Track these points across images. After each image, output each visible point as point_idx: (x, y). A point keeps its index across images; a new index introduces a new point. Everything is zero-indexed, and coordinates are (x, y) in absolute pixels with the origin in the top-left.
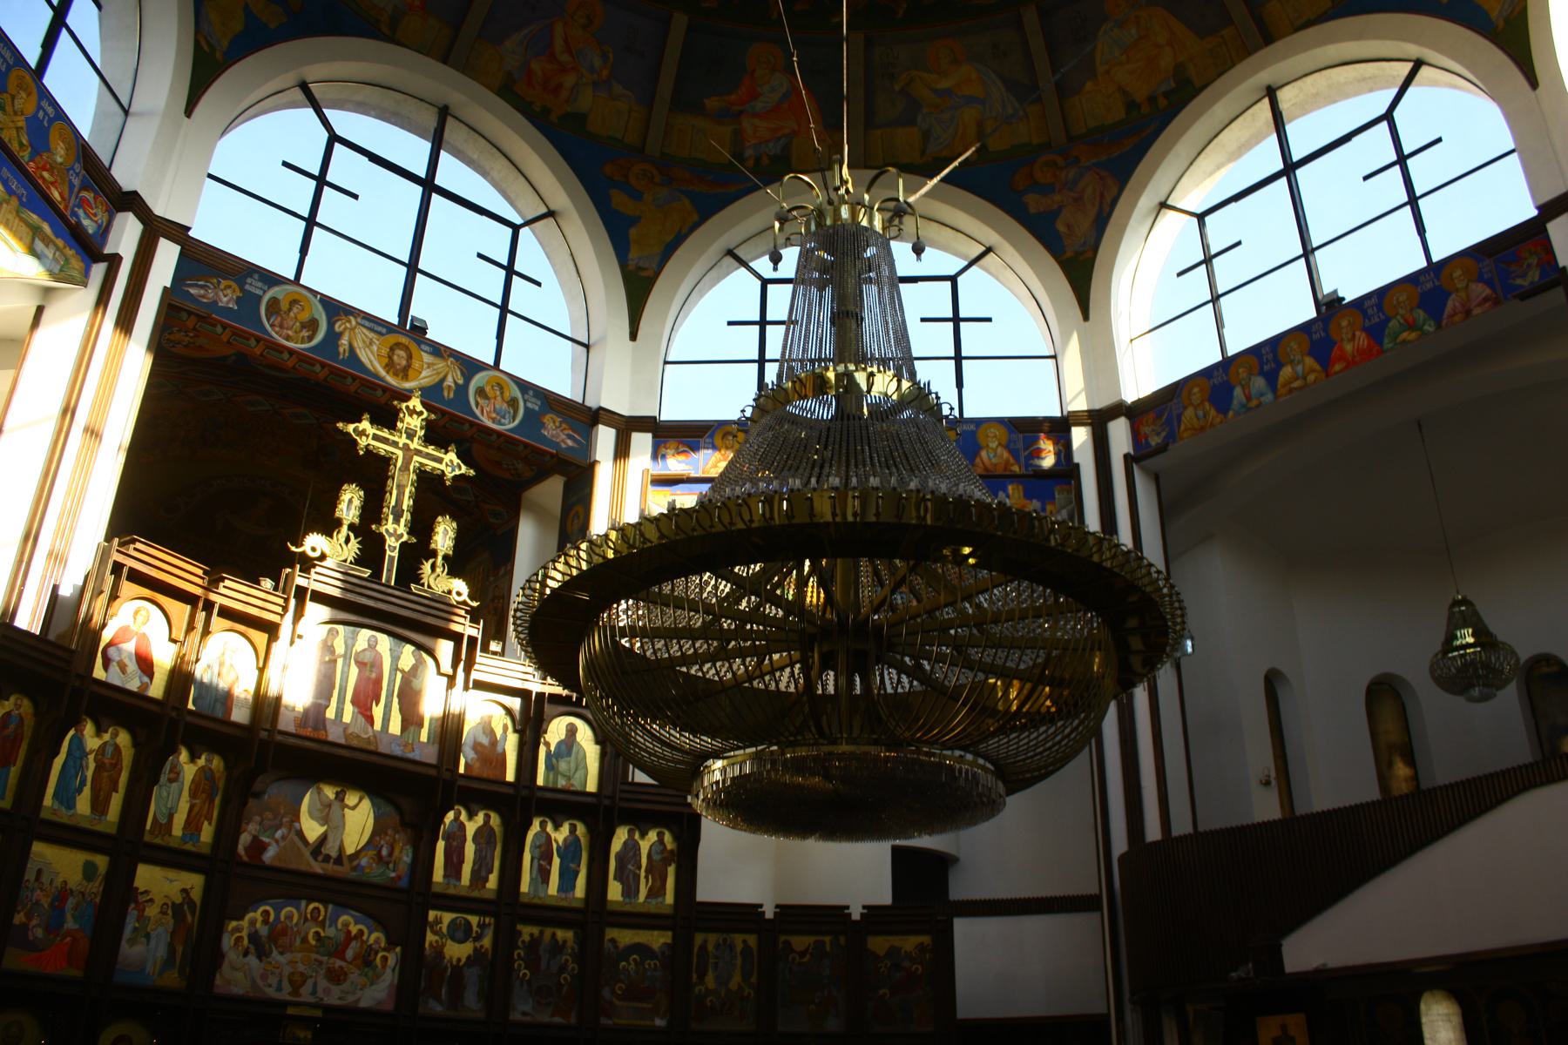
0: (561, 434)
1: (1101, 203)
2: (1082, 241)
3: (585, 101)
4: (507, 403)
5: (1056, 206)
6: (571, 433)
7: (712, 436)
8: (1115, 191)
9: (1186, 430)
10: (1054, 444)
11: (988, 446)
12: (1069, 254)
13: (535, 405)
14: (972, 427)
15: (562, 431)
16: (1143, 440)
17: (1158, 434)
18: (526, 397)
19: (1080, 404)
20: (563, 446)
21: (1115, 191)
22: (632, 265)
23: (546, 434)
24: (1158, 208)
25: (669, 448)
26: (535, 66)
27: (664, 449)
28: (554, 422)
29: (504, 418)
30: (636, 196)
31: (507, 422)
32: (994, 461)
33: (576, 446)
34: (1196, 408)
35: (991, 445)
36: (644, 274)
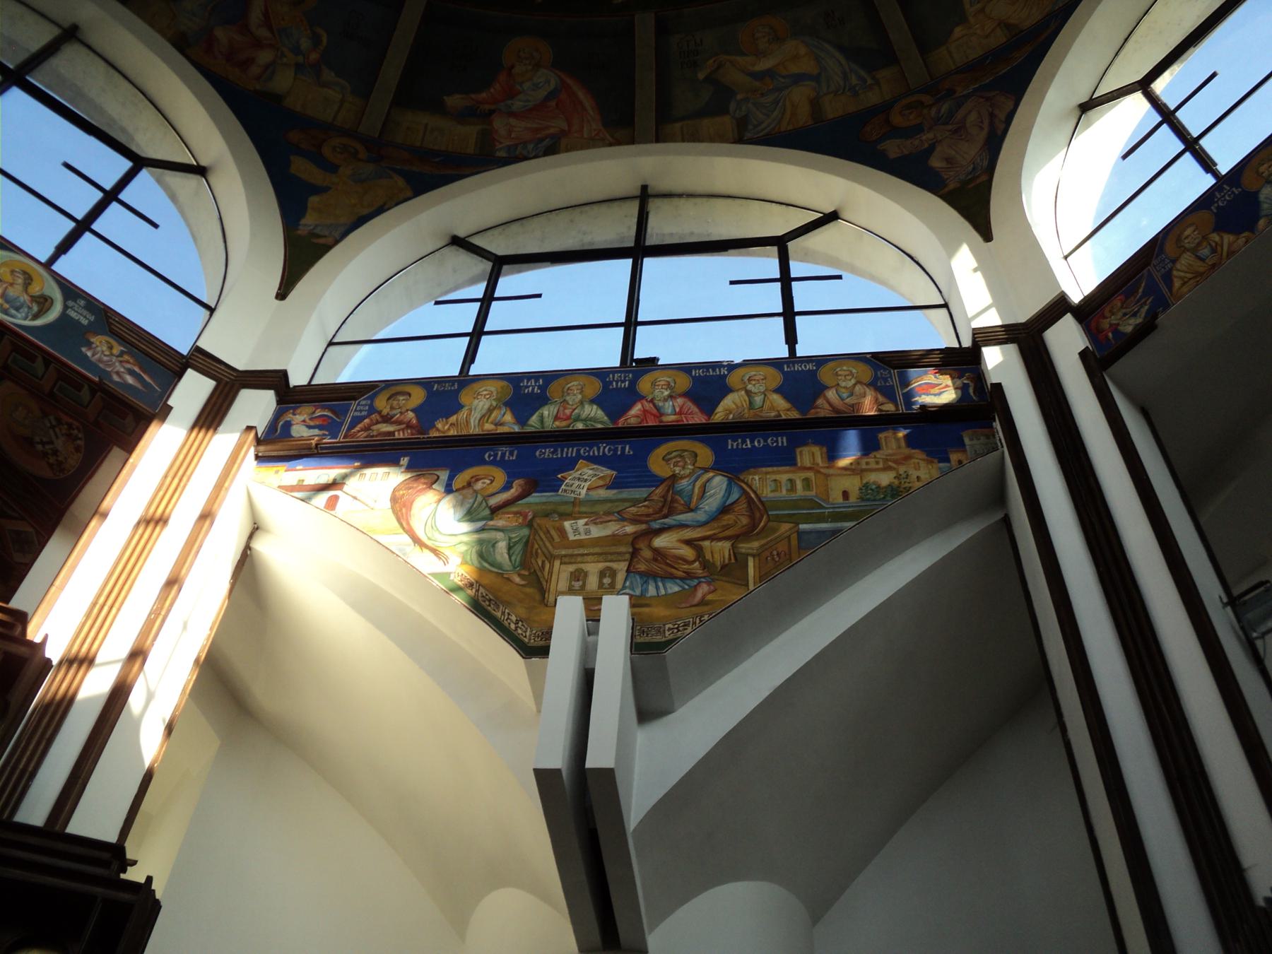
0: (117, 364)
1: (992, 124)
2: (970, 168)
3: (283, 81)
4: (31, 296)
5: (926, 145)
6: (137, 369)
7: (372, 398)
8: (1011, 104)
9: (1184, 284)
10: (953, 378)
11: (838, 384)
12: (952, 186)
13: (82, 317)
14: (810, 367)
15: (121, 362)
16: (1110, 335)
17: (1135, 315)
18: (70, 303)
19: (992, 319)
20: (116, 378)
21: (1011, 104)
22: (302, 231)
23: (89, 354)
24: (1078, 113)
25: (300, 414)
26: (221, 34)
27: (291, 415)
28: (111, 348)
29: (17, 309)
30: (332, 168)
31: (19, 315)
32: (848, 401)
33: (138, 386)
34: (1194, 251)
35: (843, 384)
36: (322, 241)
